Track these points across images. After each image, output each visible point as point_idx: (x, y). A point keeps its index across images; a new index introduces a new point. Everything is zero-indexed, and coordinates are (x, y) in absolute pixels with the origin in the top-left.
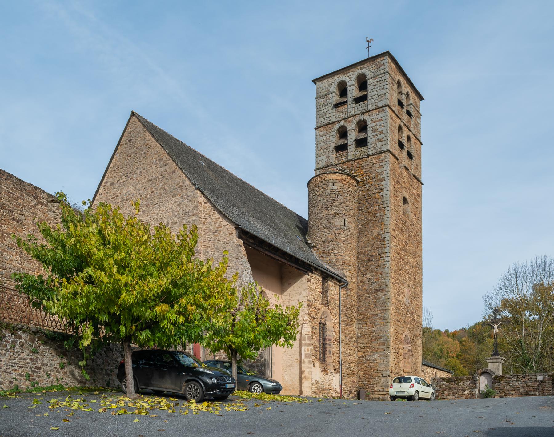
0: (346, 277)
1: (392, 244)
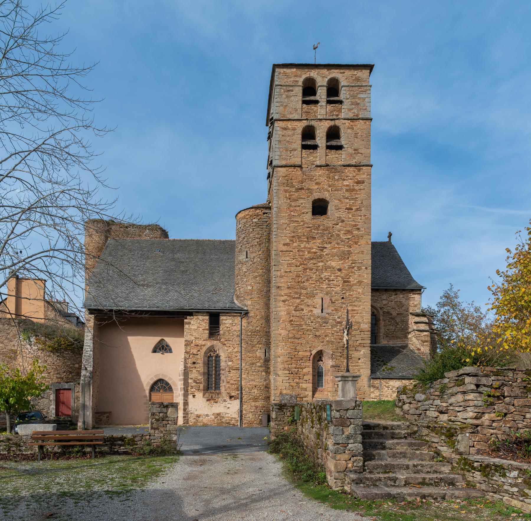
0: (247, 306)
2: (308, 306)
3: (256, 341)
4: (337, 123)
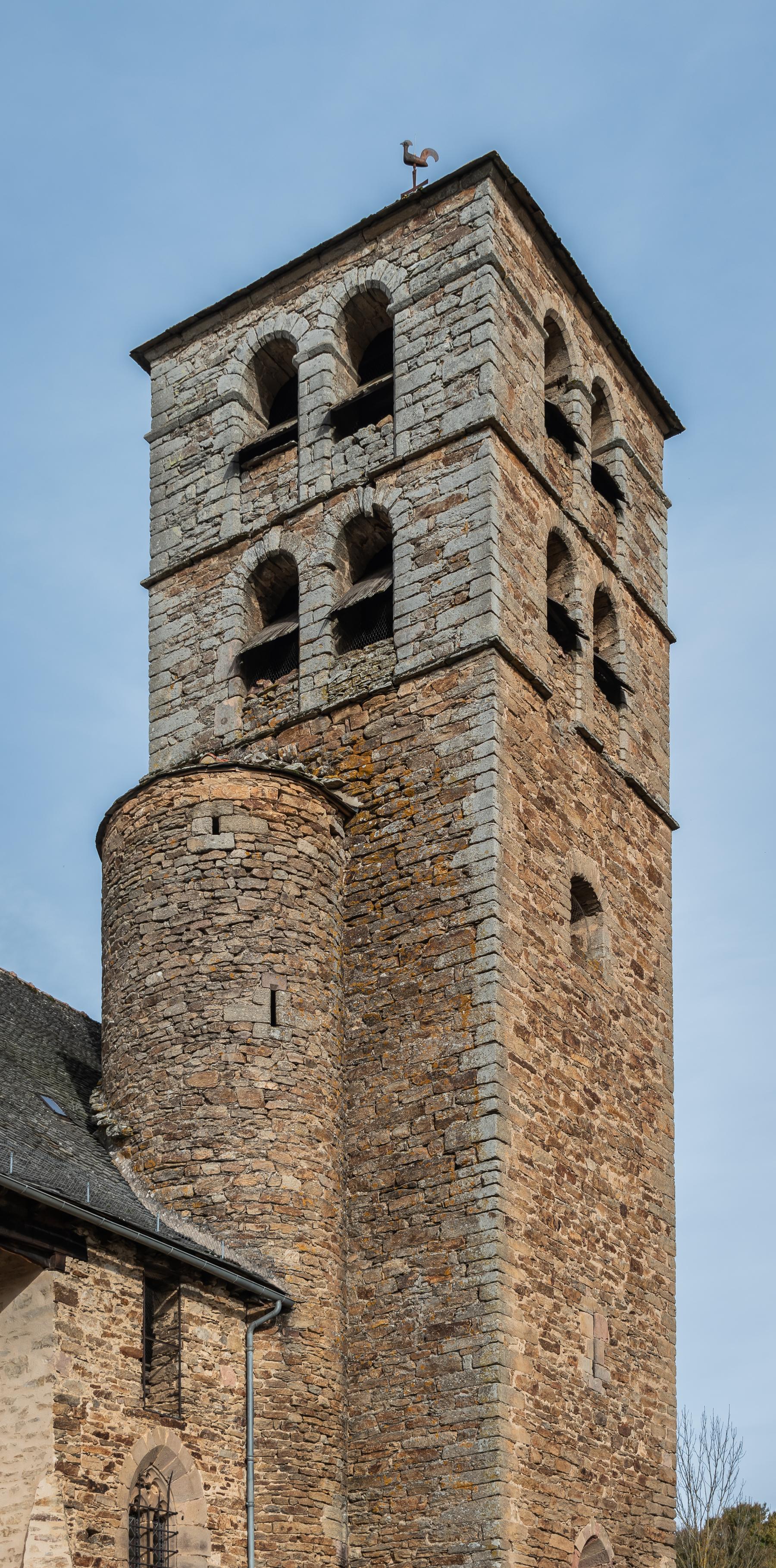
0: (281, 1275)
1: (514, 1100)
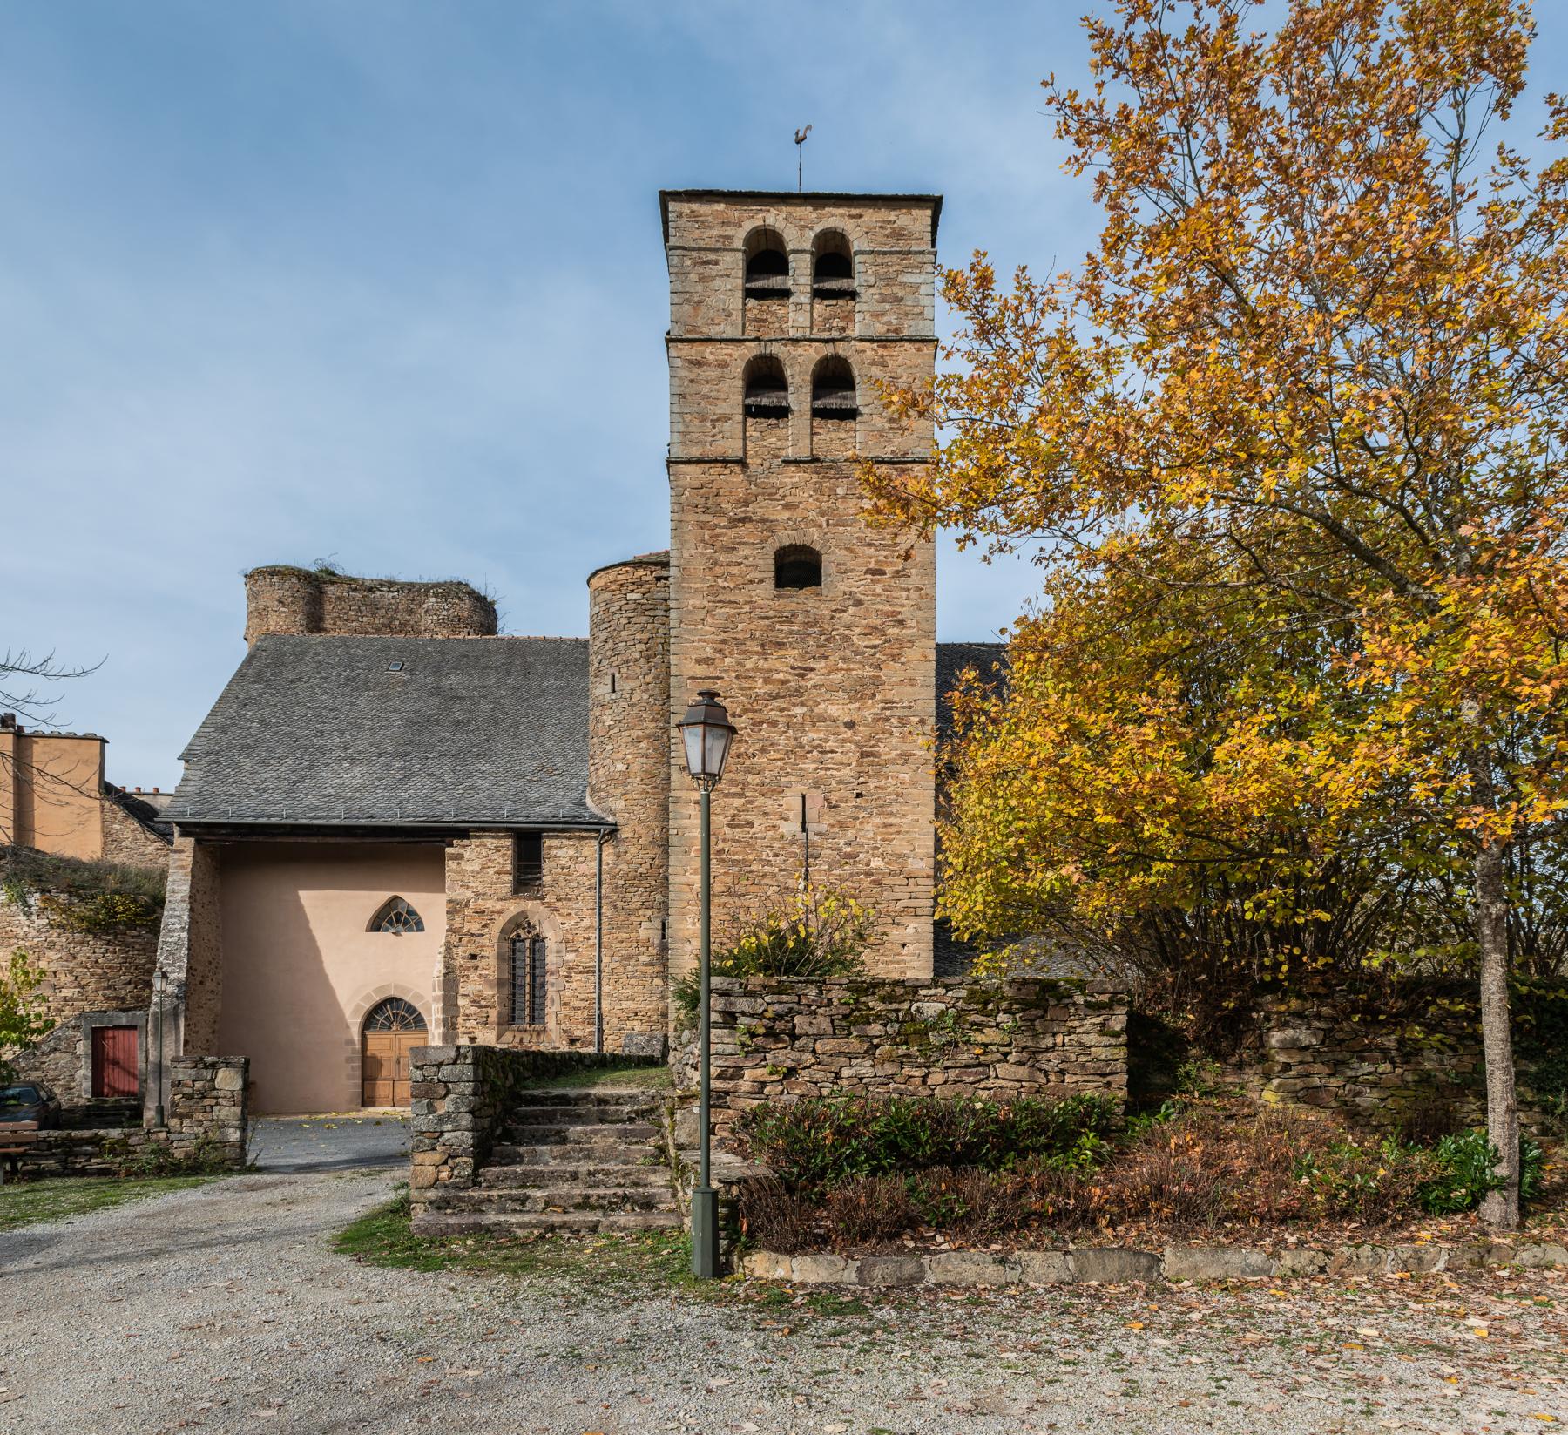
2: (766, 814)
3: (636, 901)
4: (842, 349)
